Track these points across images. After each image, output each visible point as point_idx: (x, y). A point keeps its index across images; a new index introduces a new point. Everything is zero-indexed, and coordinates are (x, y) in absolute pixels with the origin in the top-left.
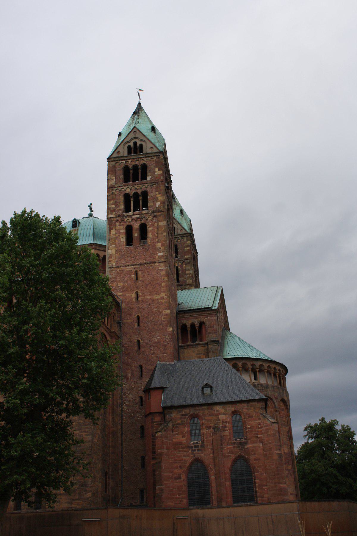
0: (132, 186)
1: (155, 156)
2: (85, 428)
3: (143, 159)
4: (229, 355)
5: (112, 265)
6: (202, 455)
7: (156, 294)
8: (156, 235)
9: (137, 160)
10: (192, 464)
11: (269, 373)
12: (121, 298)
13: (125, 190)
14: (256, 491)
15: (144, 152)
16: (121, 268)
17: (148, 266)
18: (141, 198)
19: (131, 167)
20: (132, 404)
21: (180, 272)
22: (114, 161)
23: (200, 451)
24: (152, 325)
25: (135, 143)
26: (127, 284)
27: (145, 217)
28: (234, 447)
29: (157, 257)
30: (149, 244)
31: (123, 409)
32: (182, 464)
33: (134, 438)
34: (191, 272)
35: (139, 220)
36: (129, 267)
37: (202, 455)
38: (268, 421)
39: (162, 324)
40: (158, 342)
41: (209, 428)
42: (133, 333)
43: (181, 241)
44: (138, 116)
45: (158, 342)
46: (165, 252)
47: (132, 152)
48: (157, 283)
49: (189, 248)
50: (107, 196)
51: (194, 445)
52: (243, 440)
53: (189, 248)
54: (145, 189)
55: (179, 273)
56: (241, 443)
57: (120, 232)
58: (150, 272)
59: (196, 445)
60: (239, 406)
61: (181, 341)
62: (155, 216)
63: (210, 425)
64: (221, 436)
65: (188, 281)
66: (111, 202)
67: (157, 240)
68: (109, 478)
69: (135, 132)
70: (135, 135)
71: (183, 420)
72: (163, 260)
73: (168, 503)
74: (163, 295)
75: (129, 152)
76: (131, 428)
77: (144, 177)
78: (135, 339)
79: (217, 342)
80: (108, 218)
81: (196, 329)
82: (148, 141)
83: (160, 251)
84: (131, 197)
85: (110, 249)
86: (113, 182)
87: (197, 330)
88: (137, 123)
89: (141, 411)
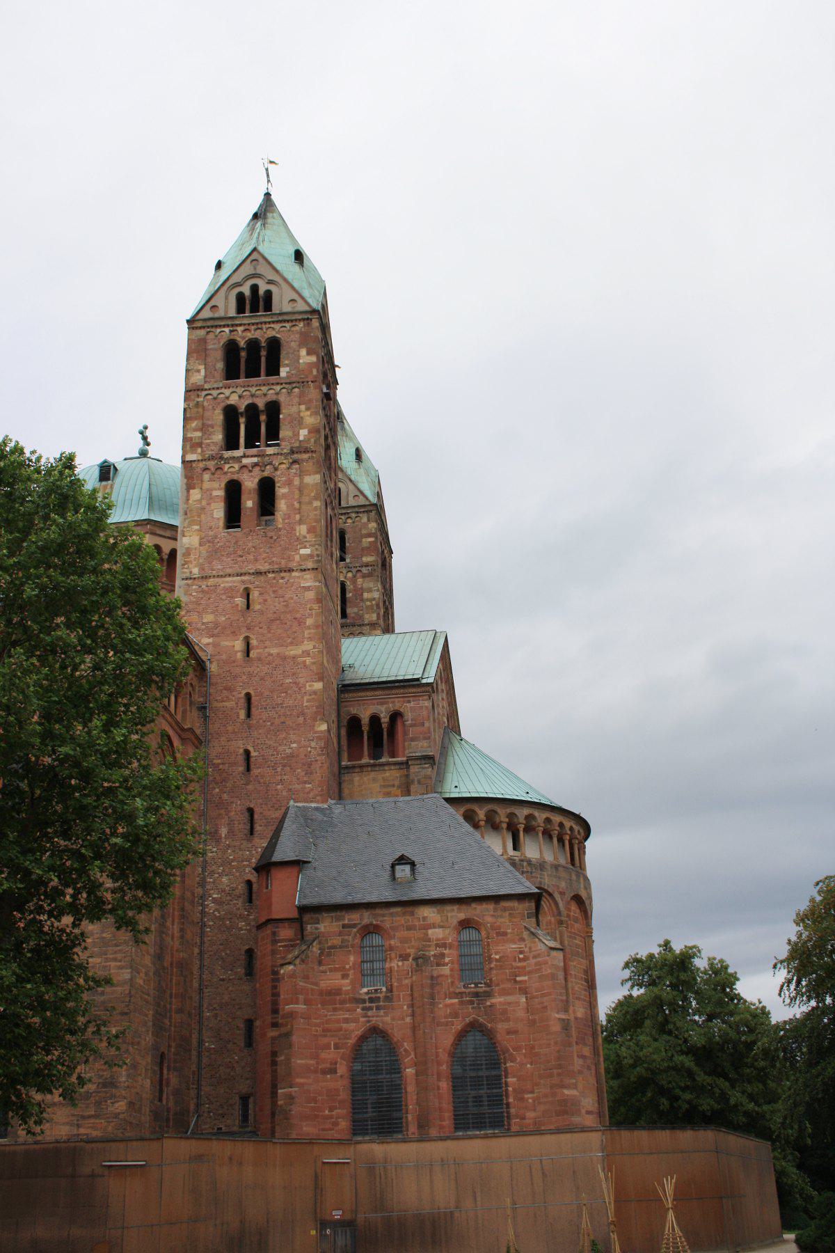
0: (243, 389)
1: (300, 320)
2: (116, 953)
3: (272, 326)
4: (457, 790)
5: (191, 572)
6: (388, 1019)
7: (292, 643)
8: (297, 505)
9: (259, 329)
10: (363, 1039)
11: (547, 834)
12: (210, 650)
13: (228, 398)
14: (508, 1105)
15: (275, 309)
16: (211, 581)
17: (274, 578)
18: (263, 418)
19: (242, 344)
20: (228, 898)
22: (204, 327)
23: (382, 1011)
24: (280, 716)
25: (255, 288)
26: (224, 619)
27: (270, 464)
28: (461, 1003)
29: (297, 558)
30: (280, 526)
31: (206, 910)
32: (339, 1039)
33: (231, 977)
34: (376, 595)
35: (257, 469)
36: (230, 579)
37: (388, 1019)
38: (542, 945)
39: (303, 714)
40: (293, 756)
41: (404, 957)
42: (234, 732)
43: (353, 522)
44: (264, 225)
45: (293, 756)
46: (317, 546)
47: (248, 307)
48: (294, 619)
49: (372, 539)
50: (185, 409)
51: (370, 996)
52: (482, 987)
53: (372, 539)
54: (274, 398)
55: (347, 596)
56: (477, 995)
57: (211, 494)
58: (280, 592)
59: (373, 996)
60: (475, 908)
61: (345, 755)
62: (295, 462)
63: (408, 950)
64: (432, 977)
65: (367, 616)
67: (298, 517)
68: (169, 1070)
69: (255, 263)
70: (255, 269)
71: (346, 937)
72: (310, 565)
73: (304, 1129)
74: (308, 646)
75: (241, 309)
76: (223, 954)
77: (274, 369)
78: (239, 746)
79: (429, 759)
80: (183, 462)
81: (382, 730)
82: (284, 285)
84: (242, 414)
85: (186, 534)
86: (199, 378)
87: (385, 730)
88: (261, 239)
89: (248, 915)
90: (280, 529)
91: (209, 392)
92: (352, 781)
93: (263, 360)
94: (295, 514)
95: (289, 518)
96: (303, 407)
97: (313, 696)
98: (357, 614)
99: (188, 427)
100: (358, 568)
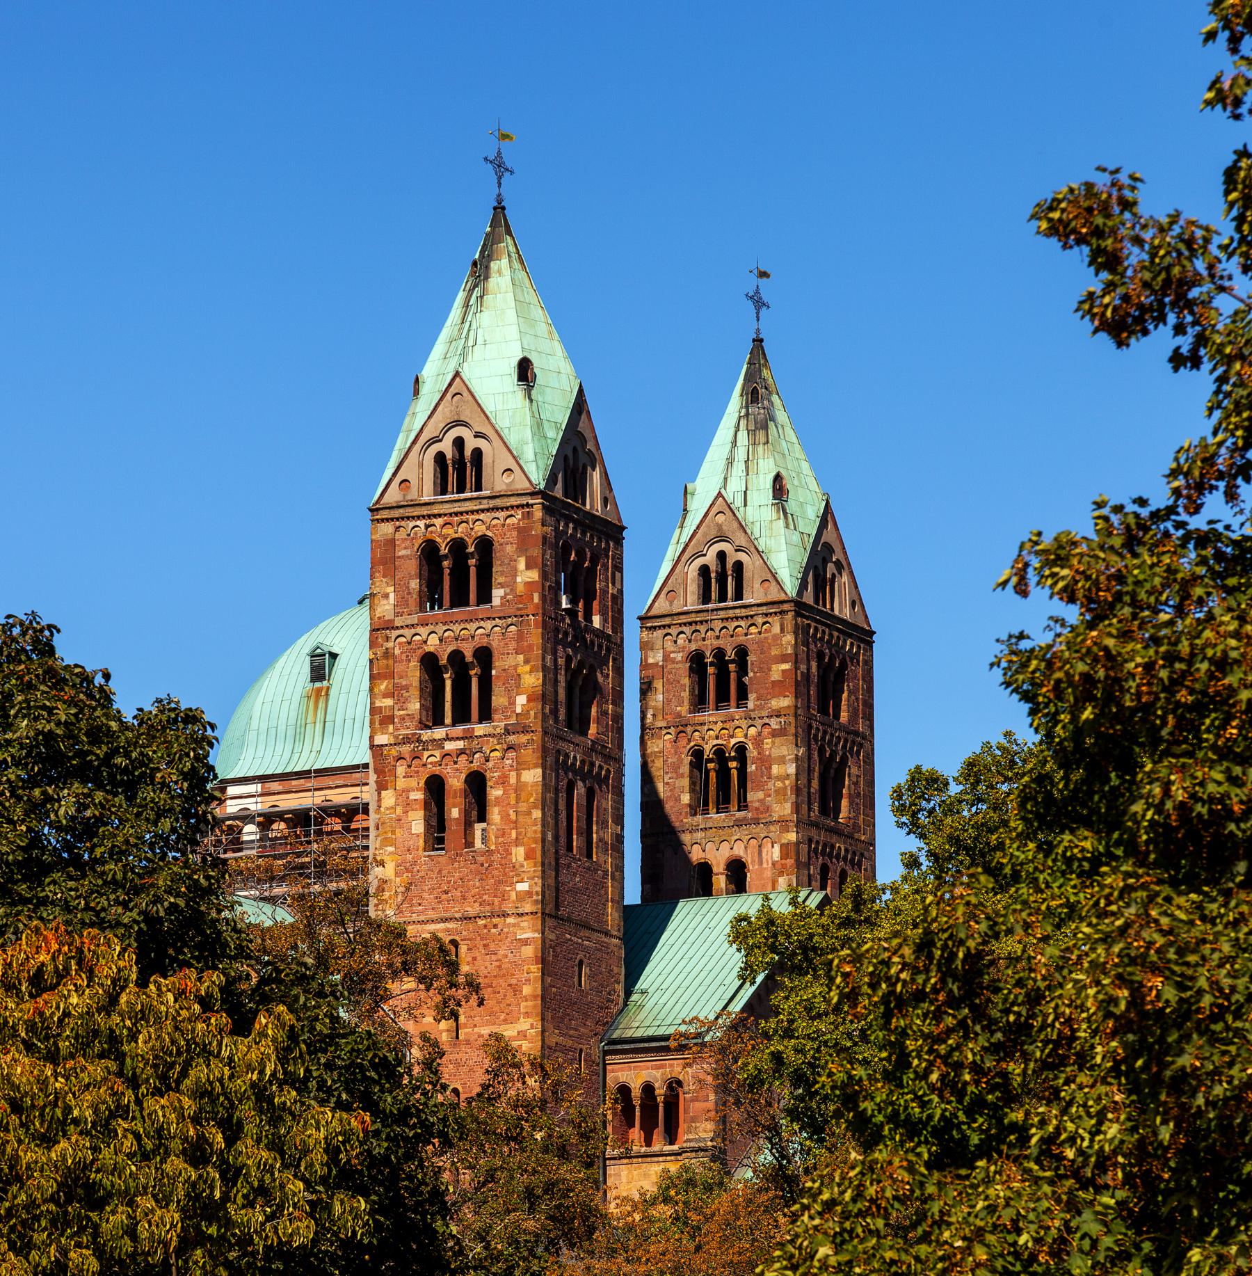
0: (445, 628)
1: (518, 507)
3: (482, 516)
7: (505, 1021)
8: (513, 816)
13: (425, 642)
17: (485, 926)
19: (444, 550)
21: (754, 767)
22: (392, 519)
25: (459, 443)
29: (513, 896)
30: (493, 847)
34: (792, 769)
35: (463, 758)
43: (760, 633)
49: (786, 666)
50: (371, 661)
53: (786, 666)
54: (484, 642)
55: (749, 770)
58: (492, 946)
62: (510, 747)
65: (776, 807)
72: (528, 907)
74: (524, 1024)
80: (372, 746)
84: (445, 666)
88: (471, 343)
92: (618, 1175)
93: (473, 571)
95: (503, 835)
96: (521, 658)
98: (761, 801)
99: (376, 690)
100: (766, 720)
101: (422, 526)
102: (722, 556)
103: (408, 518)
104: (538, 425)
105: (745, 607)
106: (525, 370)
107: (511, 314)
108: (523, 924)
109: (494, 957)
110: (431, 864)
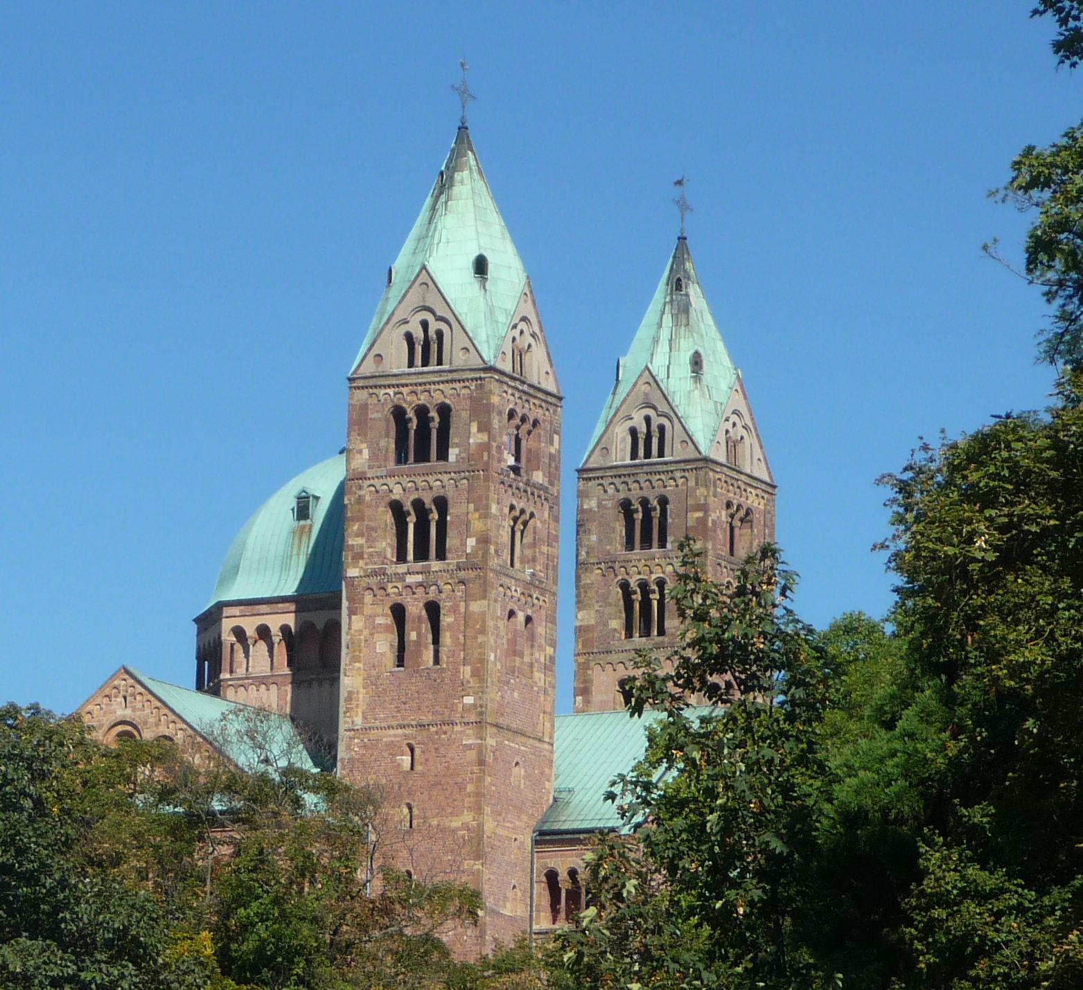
1: (472, 380)
3: (441, 386)
5: (353, 722)
8: (461, 638)
17: (437, 733)
19: (411, 414)
22: (367, 387)
30: (445, 666)
36: (392, 732)
49: (700, 514)
53: (700, 514)
57: (374, 622)
58: (442, 751)
62: (462, 582)
66: (355, 528)
72: (473, 718)
83: (469, 690)
85: (347, 674)
90: (443, 670)
91: (372, 482)
94: (460, 651)
96: (471, 506)
97: (471, 877)
101: (392, 394)
102: (648, 419)
103: (380, 387)
104: (491, 311)
105: (666, 463)
106: (481, 266)
107: (470, 217)
108: (468, 732)
109: (443, 760)
110: (392, 678)
